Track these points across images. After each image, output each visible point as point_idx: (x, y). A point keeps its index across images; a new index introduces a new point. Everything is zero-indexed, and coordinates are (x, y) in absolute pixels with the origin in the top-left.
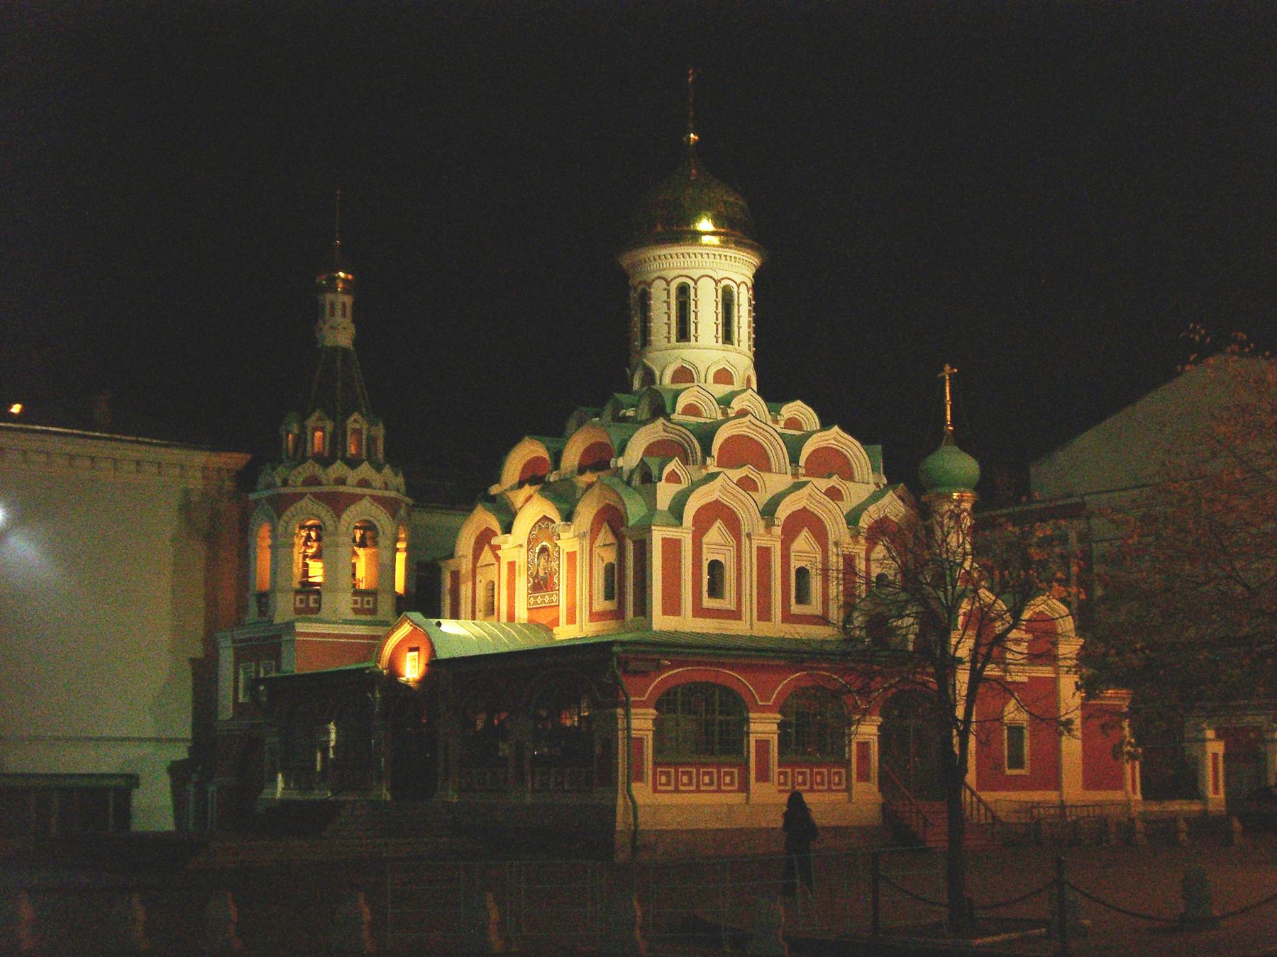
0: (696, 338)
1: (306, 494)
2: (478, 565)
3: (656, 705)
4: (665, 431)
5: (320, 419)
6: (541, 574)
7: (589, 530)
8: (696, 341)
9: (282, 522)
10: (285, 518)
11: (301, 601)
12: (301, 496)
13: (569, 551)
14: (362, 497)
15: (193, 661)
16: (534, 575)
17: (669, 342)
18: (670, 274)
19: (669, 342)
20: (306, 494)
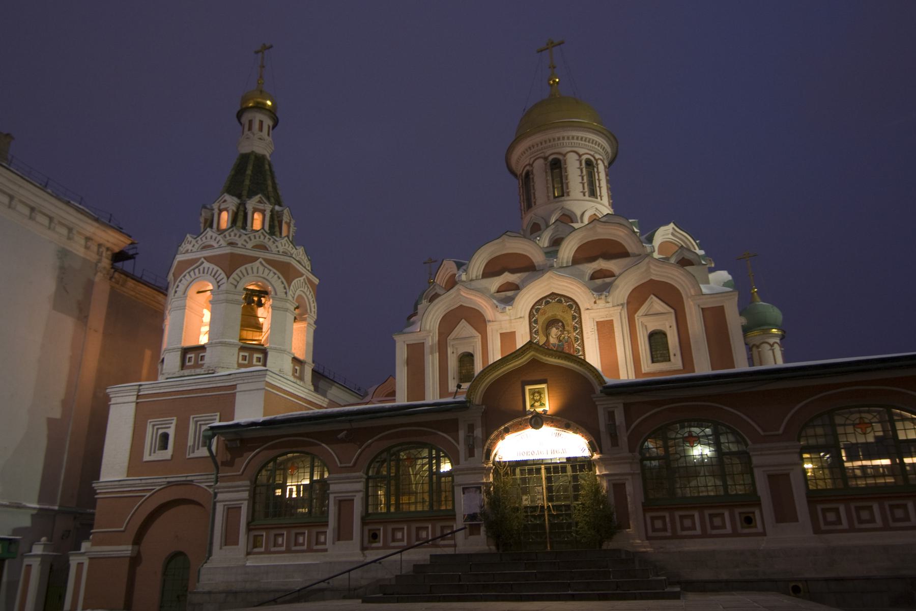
1: (256, 259)
2: (453, 335)
4: (673, 234)
5: (260, 202)
6: (553, 340)
7: (625, 301)
8: (601, 200)
9: (231, 279)
10: (234, 275)
11: (244, 358)
12: (255, 259)
13: (598, 320)
14: (302, 275)
15: (51, 422)
17: (584, 195)
18: (581, 151)
19: (584, 195)
20: (259, 258)
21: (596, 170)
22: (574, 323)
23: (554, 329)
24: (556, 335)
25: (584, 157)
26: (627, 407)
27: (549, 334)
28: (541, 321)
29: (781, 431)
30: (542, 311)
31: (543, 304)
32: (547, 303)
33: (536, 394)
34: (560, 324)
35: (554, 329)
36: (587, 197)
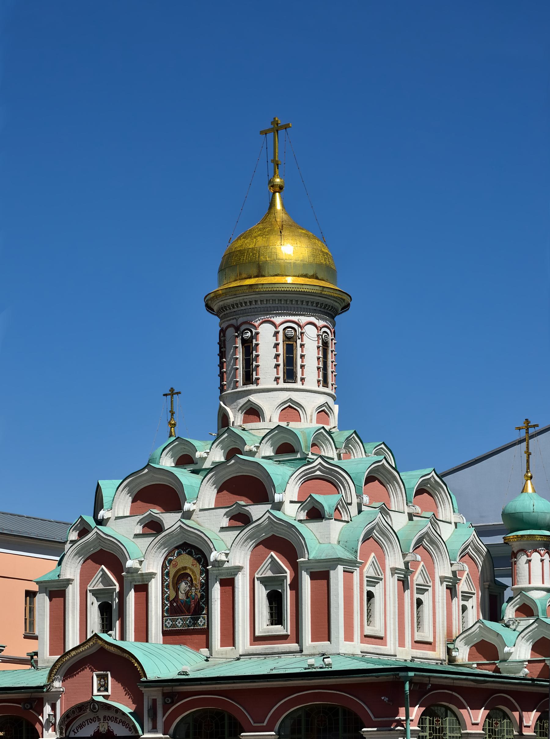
0: (302, 380)
3: (419, 724)
6: (182, 596)
8: (303, 384)
16: (171, 599)
19: (278, 383)
21: (299, 342)
22: (201, 578)
23: (183, 583)
24: (184, 591)
25: (281, 329)
26: (165, 695)
27: (179, 588)
28: (171, 575)
29: (265, 724)
30: (174, 563)
31: (175, 555)
32: (179, 554)
33: (102, 680)
34: (189, 578)
35: (183, 583)
36: (282, 385)
